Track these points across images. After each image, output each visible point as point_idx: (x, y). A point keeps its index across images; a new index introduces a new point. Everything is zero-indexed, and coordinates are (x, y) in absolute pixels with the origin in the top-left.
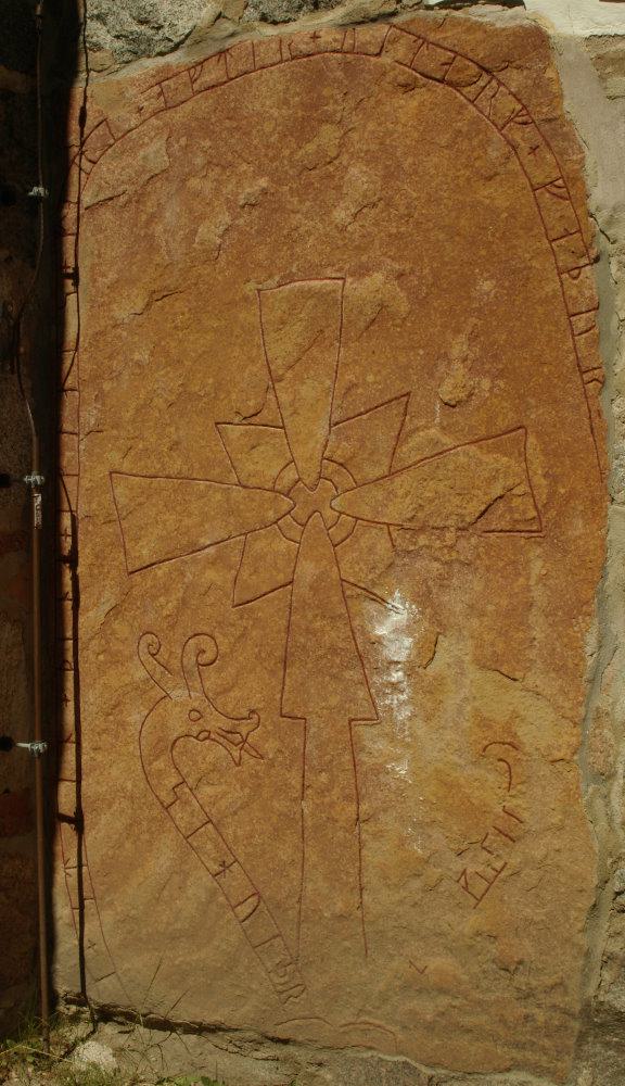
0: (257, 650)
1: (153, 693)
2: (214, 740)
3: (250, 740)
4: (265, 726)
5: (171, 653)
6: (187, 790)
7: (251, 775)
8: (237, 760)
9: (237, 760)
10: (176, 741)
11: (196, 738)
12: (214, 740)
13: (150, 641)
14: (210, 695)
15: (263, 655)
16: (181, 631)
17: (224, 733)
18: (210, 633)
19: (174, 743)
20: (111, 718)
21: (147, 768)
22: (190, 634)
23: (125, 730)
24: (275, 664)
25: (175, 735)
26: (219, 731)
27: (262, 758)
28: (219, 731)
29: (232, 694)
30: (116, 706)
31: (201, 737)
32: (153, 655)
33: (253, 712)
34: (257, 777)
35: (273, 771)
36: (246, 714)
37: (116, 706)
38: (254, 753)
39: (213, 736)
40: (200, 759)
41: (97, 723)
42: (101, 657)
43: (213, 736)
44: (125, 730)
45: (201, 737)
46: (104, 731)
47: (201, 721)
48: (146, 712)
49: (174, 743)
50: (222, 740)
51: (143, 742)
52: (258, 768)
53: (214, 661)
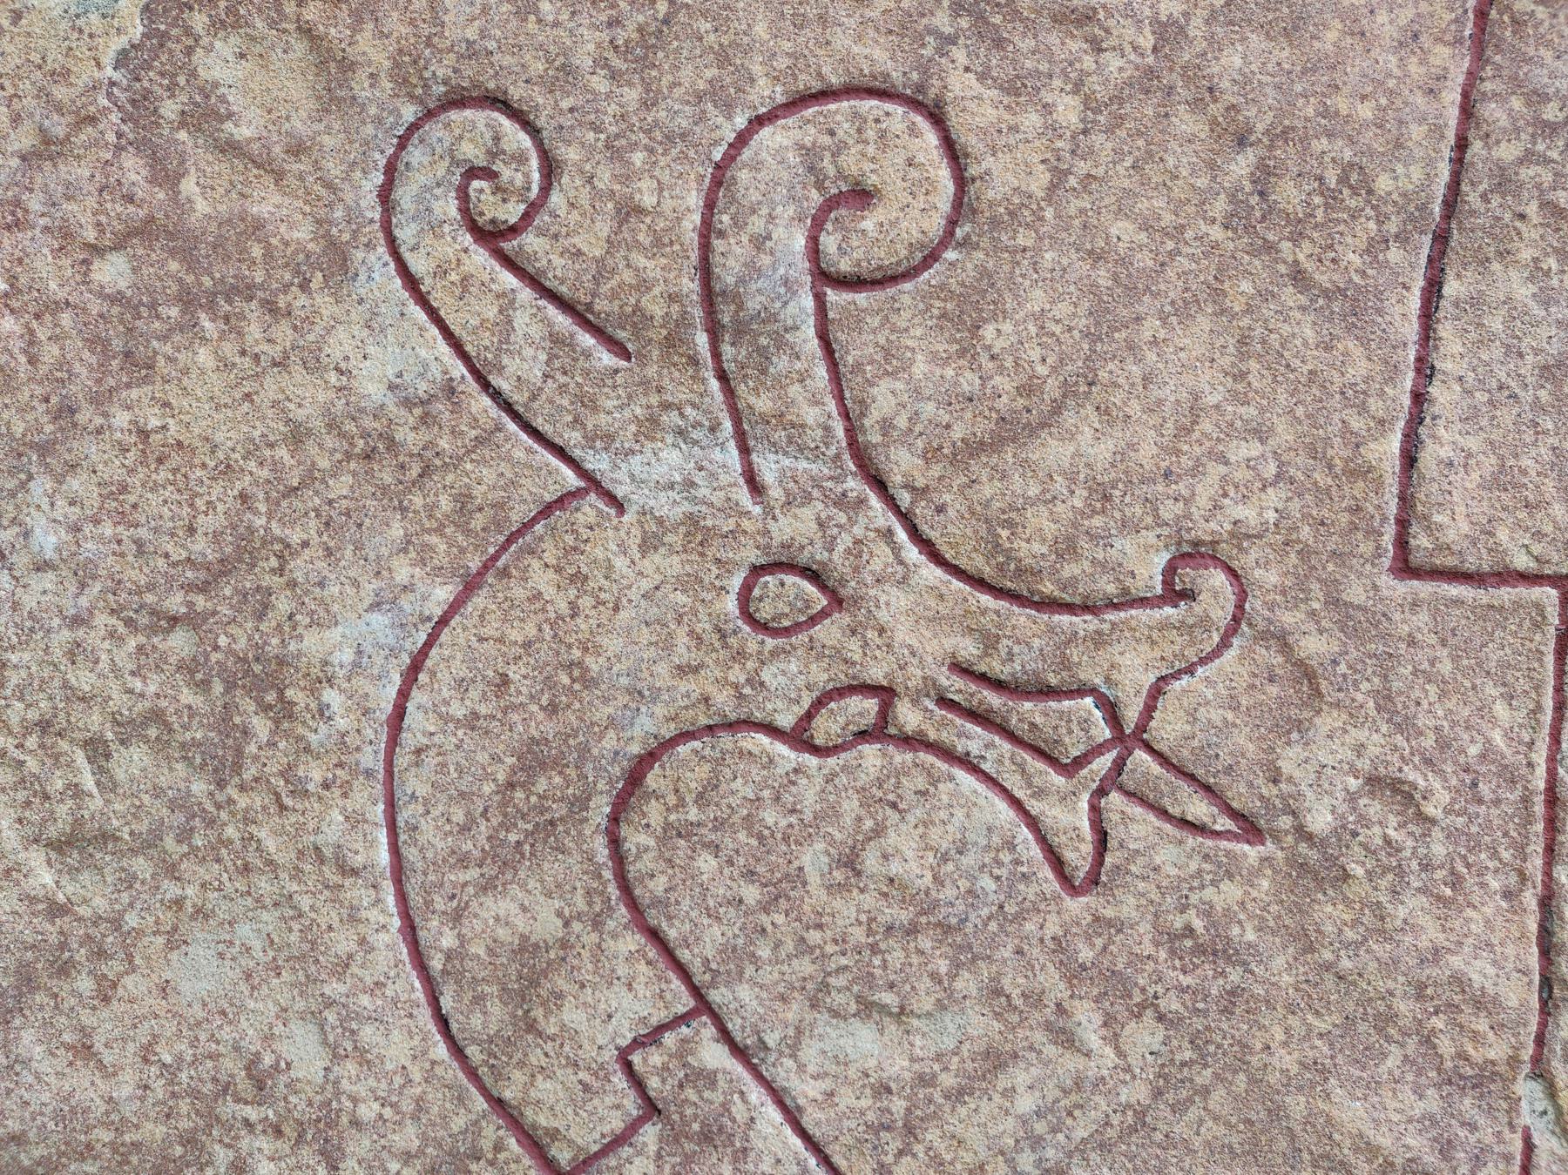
0: (1241, 166)
1: (484, 478)
2: (911, 741)
3: (1168, 728)
4: (1283, 642)
5: (629, 211)
6: (714, 1055)
7: (1173, 939)
8: (1079, 857)
9: (1079, 857)
10: (649, 759)
11: (799, 738)
12: (911, 741)
13: (471, 152)
14: (901, 464)
15: (1289, 194)
16: (695, 74)
17: (994, 699)
18: (898, 73)
19: (635, 778)
20: (180, 643)
21: (440, 938)
22: (765, 92)
23: (283, 712)
24: (1375, 247)
25: (648, 725)
26: (956, 686)
27: (1250, 829)
28: (956, 686)
29: (1053, 452)
30: (224, 569)
31: (826, 728)
32: (490, 236)
33: (1193, 554)
34: (1218, 950)
35: (1329, 914)
36: (1150, 572)
37: (224, 569)
38: (1199, 808)
39: (908, 716)
40: (813, 859)
41: (84, 680)
42: (113, 272)
43: (908, 716)
44: (283, 712)
45: (826, 728)
46: (129, 729)
47: (829, 632)
48: (443, 594)
49: (635, 778)
50: (974, 740)
51: (414, 783)
52: (1231, 892)
53: (931, 258)
